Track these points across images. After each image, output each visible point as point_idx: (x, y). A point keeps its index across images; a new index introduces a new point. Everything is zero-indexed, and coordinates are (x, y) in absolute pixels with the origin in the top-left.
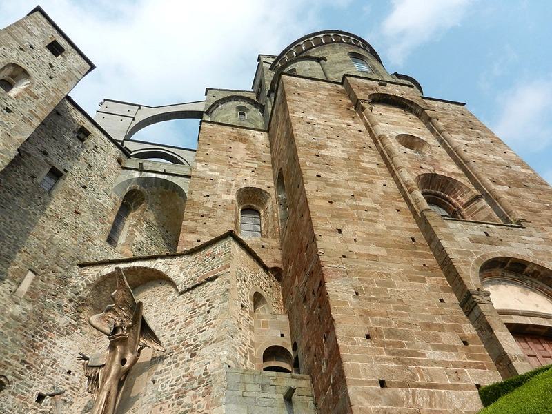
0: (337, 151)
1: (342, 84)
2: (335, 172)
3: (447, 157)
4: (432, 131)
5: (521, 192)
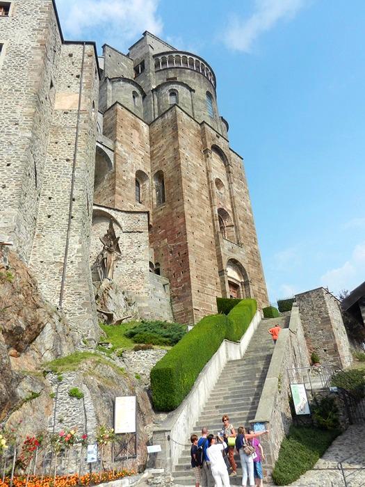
0: (194, 186)
1: (200, 124)
2: (193, 199)
3: (229, 199)
4: (228, 180)
5: (245, 225)
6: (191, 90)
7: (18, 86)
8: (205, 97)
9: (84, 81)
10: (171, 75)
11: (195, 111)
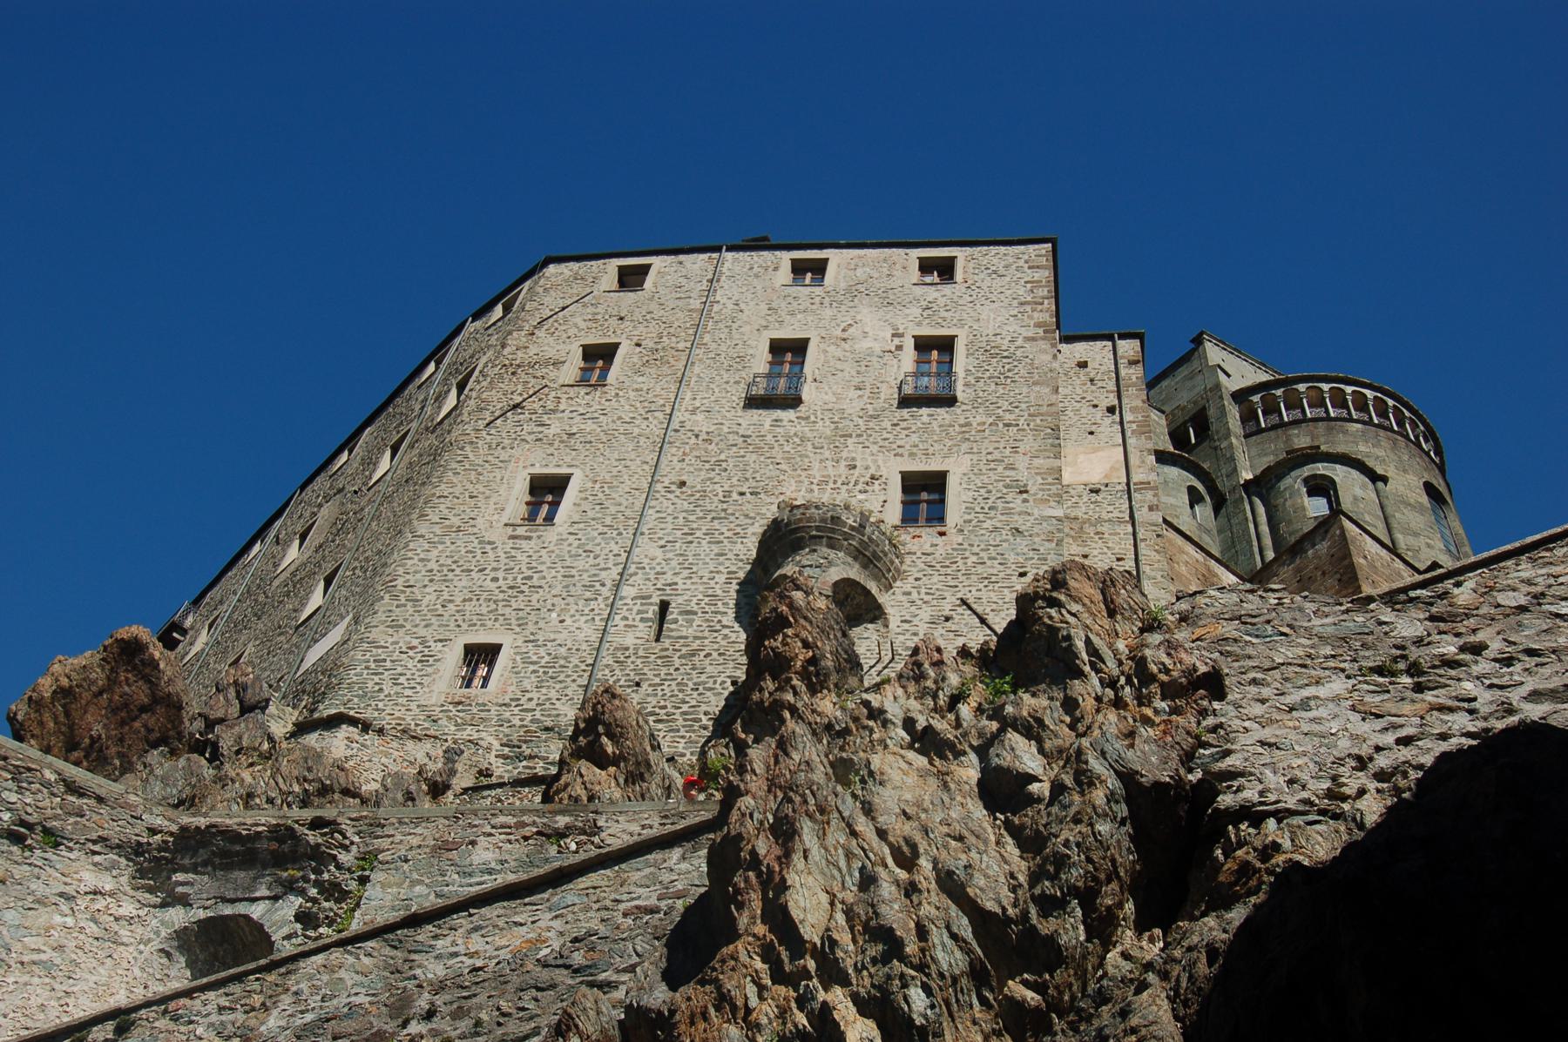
6: (1375, 477)
7: (1008, 417)
8: (1425, 499)
9: (1128, 417)
10: (1301, 440)
11: (1399, 537)
